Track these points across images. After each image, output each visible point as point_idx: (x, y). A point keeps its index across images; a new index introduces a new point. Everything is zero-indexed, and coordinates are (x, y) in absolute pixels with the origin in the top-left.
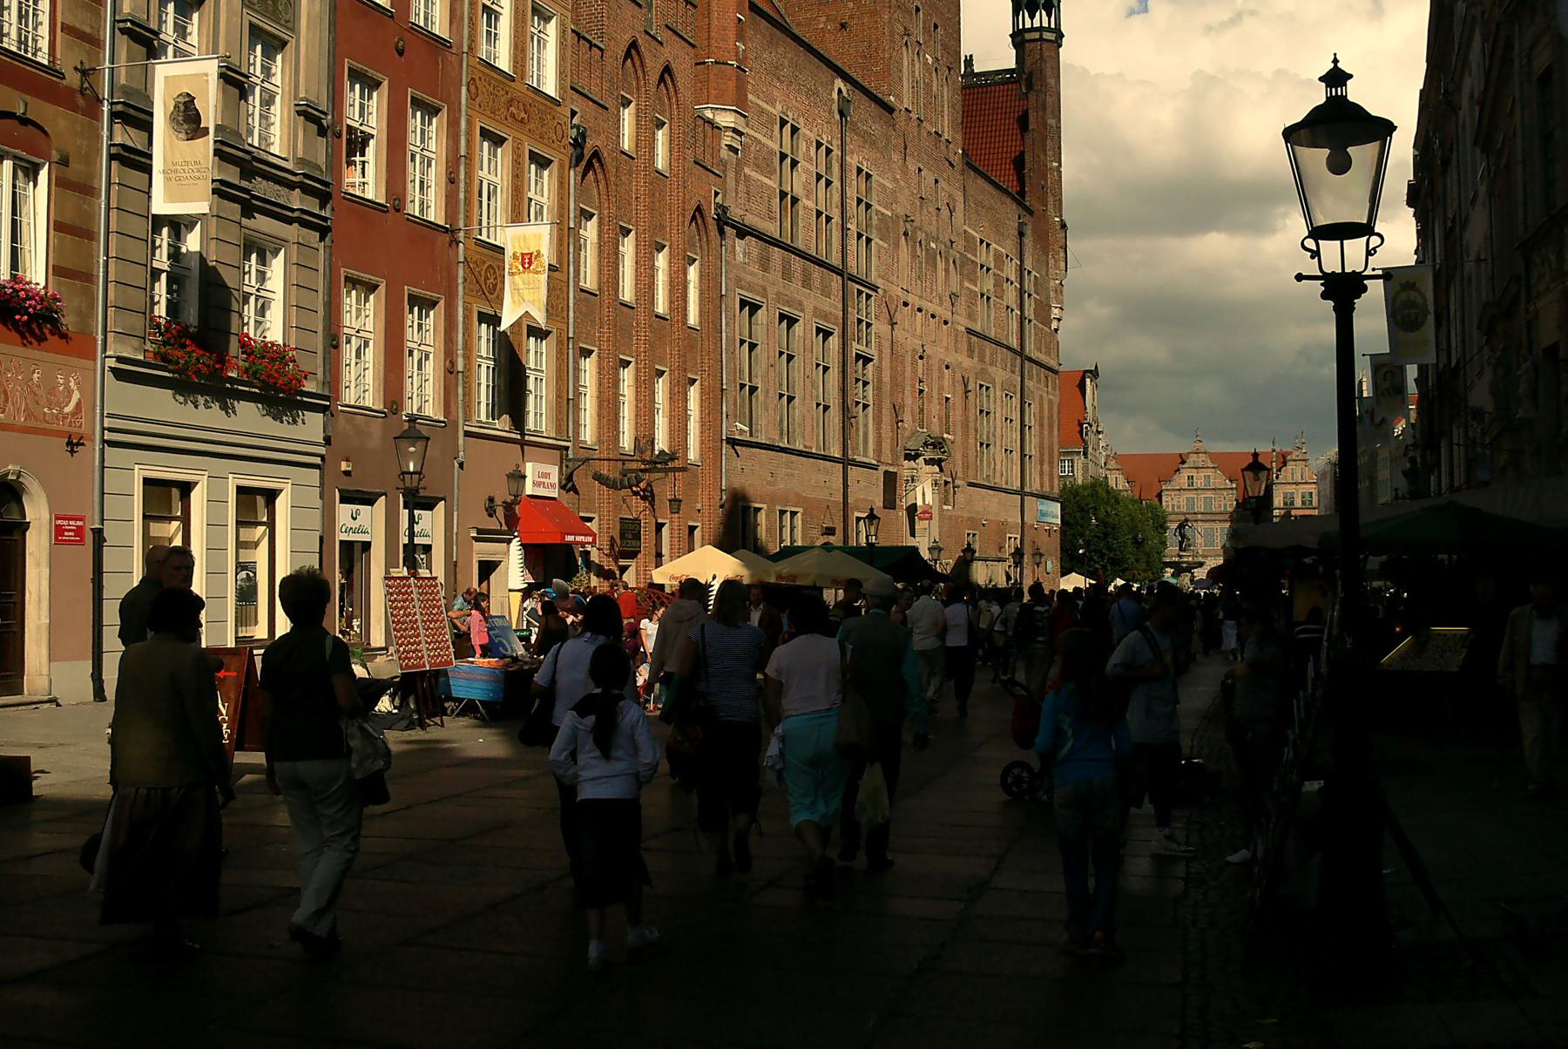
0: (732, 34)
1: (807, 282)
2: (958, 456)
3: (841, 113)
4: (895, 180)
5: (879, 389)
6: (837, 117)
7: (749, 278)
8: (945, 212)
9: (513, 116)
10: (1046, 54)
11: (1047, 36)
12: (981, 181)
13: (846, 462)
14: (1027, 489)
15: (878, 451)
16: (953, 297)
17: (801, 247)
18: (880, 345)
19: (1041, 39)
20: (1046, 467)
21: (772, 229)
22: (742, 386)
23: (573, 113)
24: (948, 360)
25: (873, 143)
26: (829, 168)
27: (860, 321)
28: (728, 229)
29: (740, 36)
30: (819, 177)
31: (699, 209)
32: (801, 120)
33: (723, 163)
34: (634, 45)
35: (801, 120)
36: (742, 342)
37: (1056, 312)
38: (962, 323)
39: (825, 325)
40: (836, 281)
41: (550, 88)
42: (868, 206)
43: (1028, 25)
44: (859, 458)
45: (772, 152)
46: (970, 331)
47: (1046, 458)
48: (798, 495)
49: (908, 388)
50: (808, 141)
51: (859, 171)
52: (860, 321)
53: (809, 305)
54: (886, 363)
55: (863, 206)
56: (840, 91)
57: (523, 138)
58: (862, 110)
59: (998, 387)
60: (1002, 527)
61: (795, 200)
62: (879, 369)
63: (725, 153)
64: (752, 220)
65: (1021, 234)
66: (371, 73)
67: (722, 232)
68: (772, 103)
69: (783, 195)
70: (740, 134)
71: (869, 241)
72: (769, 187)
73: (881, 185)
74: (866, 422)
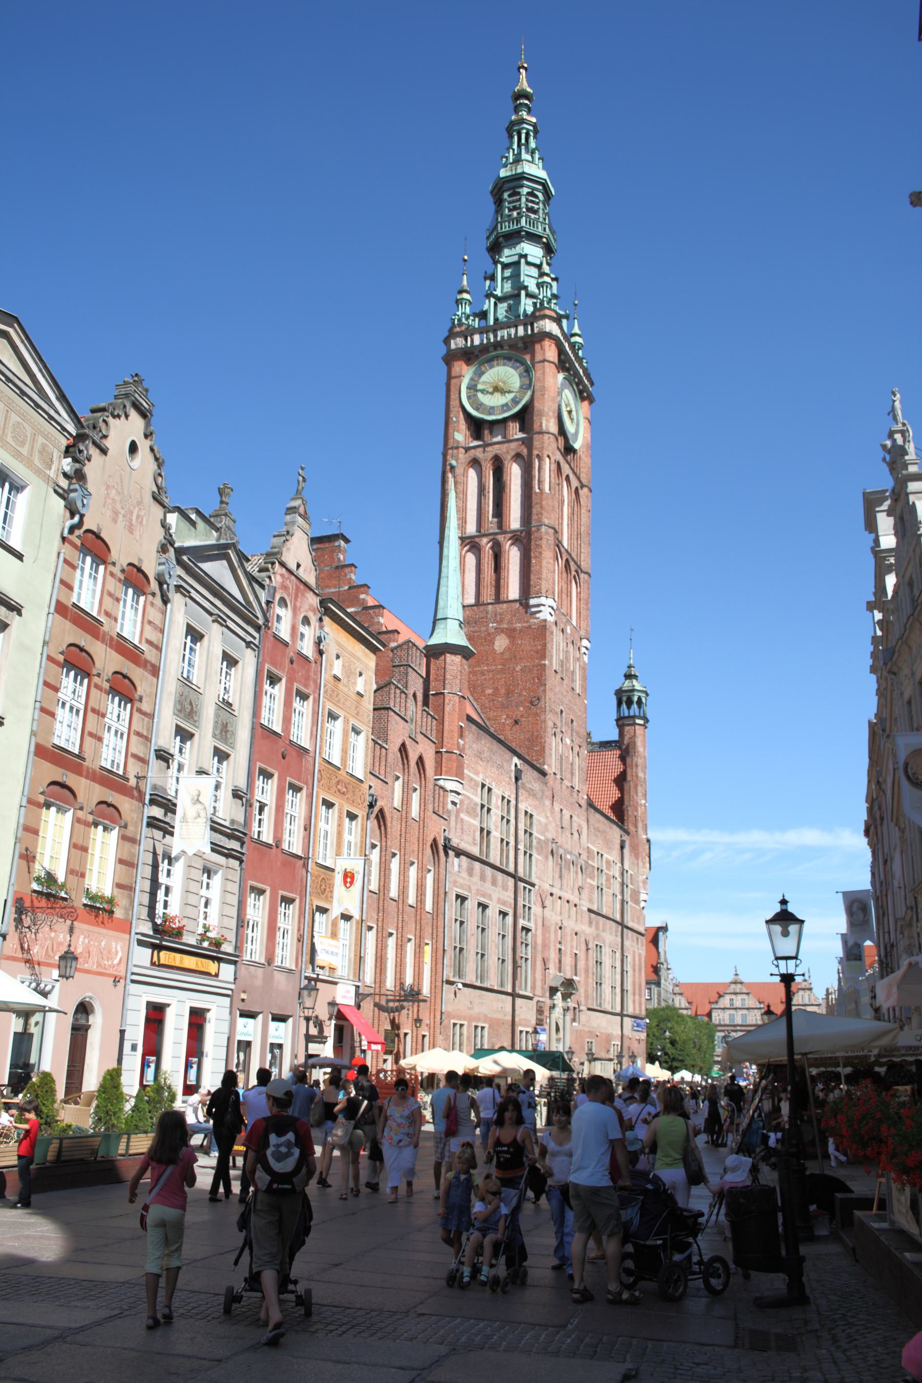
0: (456, 735)
1: (494, 883)
2: (582, 990)
3: (517, 779)
4: (547, 817)
6: (514, 780)
7: (461, 881)
8: (576, 835)
9: (339, 791)
10: (638, 732)
11: (638, 721)
12: (598, 816)
13: (514, 995)
14: (625, 1013)
15: (534, 988)
16: (580, 889)
17: (492, 861)
18: (536, 921)
19: (635, 724)
20: (637, 997)
21: (475, 851)
22: (455, 947)
23: (370, 787)
24: (577, 929)
25: (534, 795)
26: (508, 812)
27: (524, 906)
28: (451, 853)
29: (461, 736)
30: (503, 818)
31: (435, 840)
32: (494, 784)
33: (449, 812)
34: (403, 746)
35: (494, 784)
36: (456, 920)
37: (643, 896)
39: (504, 909)
40: (511, 881)
41: (360, 774)
42: (531, 834)
43: (626, 714)
44: (522, 993)
45: (476, 804)
46: (590, 911)
47: (637, 991)
48: (486, 1016)
49: (552, 948)
50: (497, 796)
51: (526, 812)
52: (524, 906)
53: (495, 896)
54: (539, 932)
55: (528, 834)
56: (516, 765)
57: (344, 803)
58: (529, 775)
59: (607, 945)
60: (609, 1038)
61: (489, 833)
62: (535, 936)
64: (464, 846)
65: (622, 847)
66: (270, 770)
67: (447, 854)
68: (477, 773)
69: (482, 829)
70: (458, 794)
71: (531, 855)
72: (474, 825)
73: (539, 821)
74: (526, 970)
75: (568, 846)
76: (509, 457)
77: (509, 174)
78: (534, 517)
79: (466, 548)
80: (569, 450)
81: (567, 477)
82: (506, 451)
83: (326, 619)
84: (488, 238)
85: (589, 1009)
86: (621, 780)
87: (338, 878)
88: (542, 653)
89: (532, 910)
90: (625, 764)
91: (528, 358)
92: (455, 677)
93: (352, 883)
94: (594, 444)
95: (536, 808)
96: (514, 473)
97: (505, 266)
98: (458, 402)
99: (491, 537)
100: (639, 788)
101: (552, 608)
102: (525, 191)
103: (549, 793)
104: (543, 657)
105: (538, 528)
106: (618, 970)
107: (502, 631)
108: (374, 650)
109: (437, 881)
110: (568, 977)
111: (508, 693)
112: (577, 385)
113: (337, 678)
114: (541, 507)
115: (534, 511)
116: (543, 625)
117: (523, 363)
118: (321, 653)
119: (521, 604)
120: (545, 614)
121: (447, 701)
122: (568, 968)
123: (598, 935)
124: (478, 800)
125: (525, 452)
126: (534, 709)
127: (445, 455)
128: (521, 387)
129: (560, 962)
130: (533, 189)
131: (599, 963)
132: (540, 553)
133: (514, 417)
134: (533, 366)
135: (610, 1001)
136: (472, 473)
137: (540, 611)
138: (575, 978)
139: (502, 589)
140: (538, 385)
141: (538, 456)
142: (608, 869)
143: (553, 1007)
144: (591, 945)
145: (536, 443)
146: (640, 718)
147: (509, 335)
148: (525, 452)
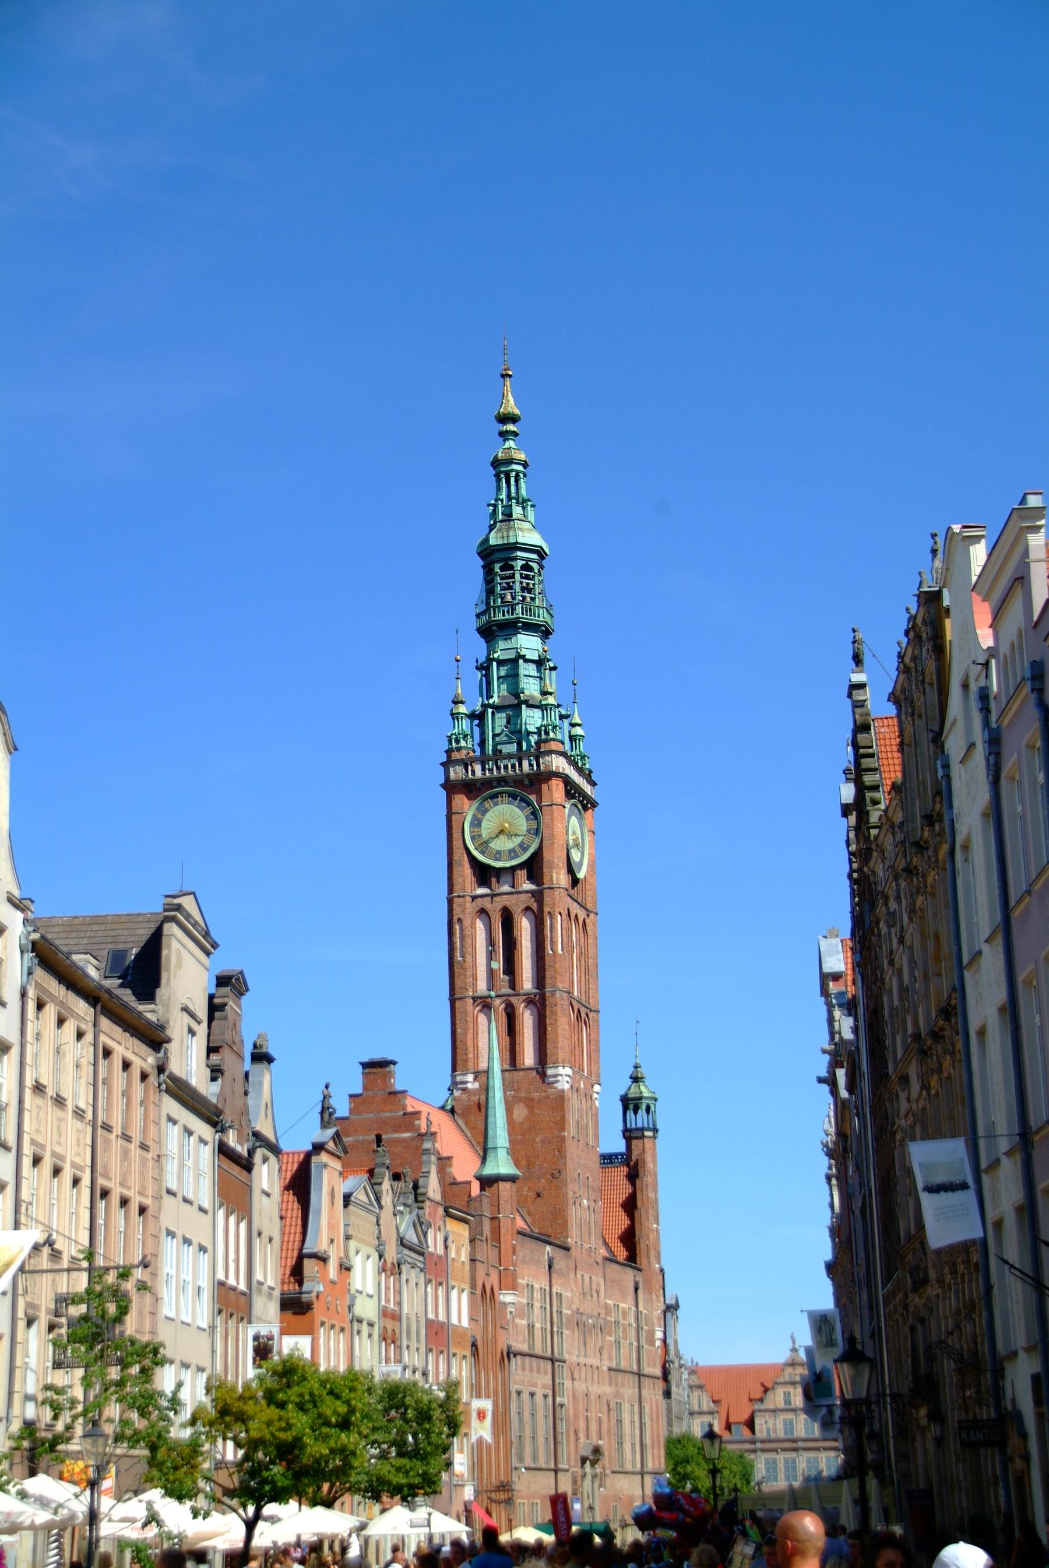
0: (510, 1253)
2: (606, 1453)
3: (550, 1267)
5: (567, 1422)
8: (595, 1295)
13: (556, 1471)
15: (569, 1460)
19: (643, 1137)
20: (656, 1450)
21: (524, 1348)
24: (599, 1392)
38: (605, 1365)
43: (634, 1126)
44: (561, 1466)
46: (610, 1369)
53: (539, 1384)
54: (571, 1405)
62: (567, 1410)
63: (509, 1316)
65: (636, 1289)
68: (523, 1278)
73: (567, 1297)
75: (589, 1311)
76: (519, 910)
77: (500, 542)
78: (548, 981)
81: (576, 916)
82: (516, 904)
83: (447, 1219)
84: (478, 616)
85: (613, 1472)
86: (630, 1206)
87: (474, 1415)
88: (562, 1125)
89: (565, 1386)
91: (533, 798)
92: (507, 1202)
93: (484, 1417)
95: (563, 1285)
96: (524, 928)
97: (501, 663)
99: (504, 998)
100: (651, 1211)
102: (520, 563)
103: (572, 1266)
104: (563, 1129)
105: (553, 993)
106: (637, 1424)
107: (520, 1100)
109: (504, 1383)
110: (594, 1443)
112: (581, 802)
113: (453, 1259)
116: (561, 1097)
117: (529, 804)
118: (446, 1247)
119: (538, 1072)
122: (594, 1433)
123: (618, 1392)
124: (524, 1301)
125: (535, 906)
126: (555, 1182)
128: (529, 831)
129: (587, 1429)
130: (528, 560)
131: (620, 1422)
133: (520, 866)
135: (631, 1460)
136: (480, 925)
138: (600, 1442)
139: (518, 1056)
140: (546, 832)
142: (624, 1319)
143: (584, 1476)
144: (612, 1405)
145: (547, 899)
146: (648, 1129)
147: (513, 766)
148: (535, 906)
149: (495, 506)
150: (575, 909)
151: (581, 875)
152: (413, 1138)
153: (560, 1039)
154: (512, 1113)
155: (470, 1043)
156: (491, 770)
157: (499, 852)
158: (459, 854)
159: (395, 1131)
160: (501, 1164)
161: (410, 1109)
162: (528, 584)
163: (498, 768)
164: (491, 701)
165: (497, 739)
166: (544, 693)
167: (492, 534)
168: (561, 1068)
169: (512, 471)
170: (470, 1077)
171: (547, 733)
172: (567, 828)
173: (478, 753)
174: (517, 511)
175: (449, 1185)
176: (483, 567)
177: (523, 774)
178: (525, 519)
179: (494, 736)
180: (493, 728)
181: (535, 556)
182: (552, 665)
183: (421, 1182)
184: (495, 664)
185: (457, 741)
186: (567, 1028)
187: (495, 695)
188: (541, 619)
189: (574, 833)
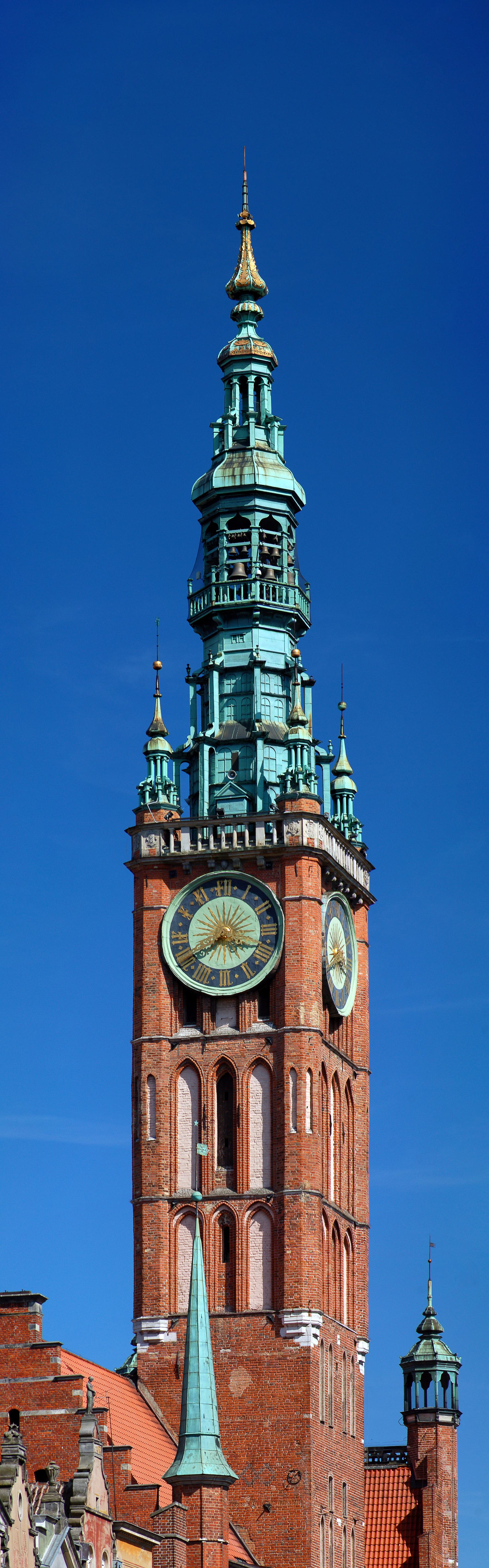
10: (442, 1438)
11: (442, 1418)
43: (421, 1406)
76: (246, 1065)
78: (288, 1177)
79: (177, 1217)
80: (335, 1021)
81: (336, 1074)
82: (242, 1054)
88: (304, 1401)
90: (419, 1497)
91: (271, 887)
94: (376, 991)
96: (253, 1092)
97: (226, 673)
98: (156, 955)
100: (445, 1539)
101: (318, 1327)
102: (260, 517)
104: (306, 1408)
105: (296, 1196)
107: (241, 1361)
108: (148, 1546)
111: (253, 1463)
112: (348, 895)
114: (300, 1161)
115: (288, 1166)
116: (305, 1357)
117: (264, 896)
119: (270, 1320)
120: (309, 1339)
121: (205, 1553)
127: (137, 1050)
128: (263, 939)
130: (272, 512)
132: (299, 1238)
134: (283, 904)
136: (182, 1085)
137: (300, 1334)
139: (238, 1292)
140: (291, 942)
141: (293, 1069)
145: (290, 1048)
147: (241, 836)
148: (270, 1059)
149: (223, 427)
150: (335, 1064)
151: (345, 1011)
152: (68, 1417)
153: (305, 1269)
154: (228, 1382)
155: (164, 1271)
156: (206, 842)
157: (215, 972)
158: (153, 973)
159: (41, 1406)
160: (206, 1459)
161: (65, 1372)
162: (271, 550)
163: (217, 839)
164: (208, 733)
165: (217, 793)
166: (293, 722)
167: (217, 472)
168: (305, 1315)
169: (251, 373)
170: (163, 1325)
171: (295, 785)
172: (325, 934)
173: (187, 813)
174: (257, 435)
175: (125, 1490)
176: (203, 523)
177: (255, 849)
178: (269, 449)
179: (212, 788)
180: (211, 776)
181: (283, 507)
182: (306, 677)
183: (77, 1484)
184: (216, 674)
185: (154, 795)
186: (317, 1251)
187: (216, 724)
188: (291, 605)
189: (335, 944)
